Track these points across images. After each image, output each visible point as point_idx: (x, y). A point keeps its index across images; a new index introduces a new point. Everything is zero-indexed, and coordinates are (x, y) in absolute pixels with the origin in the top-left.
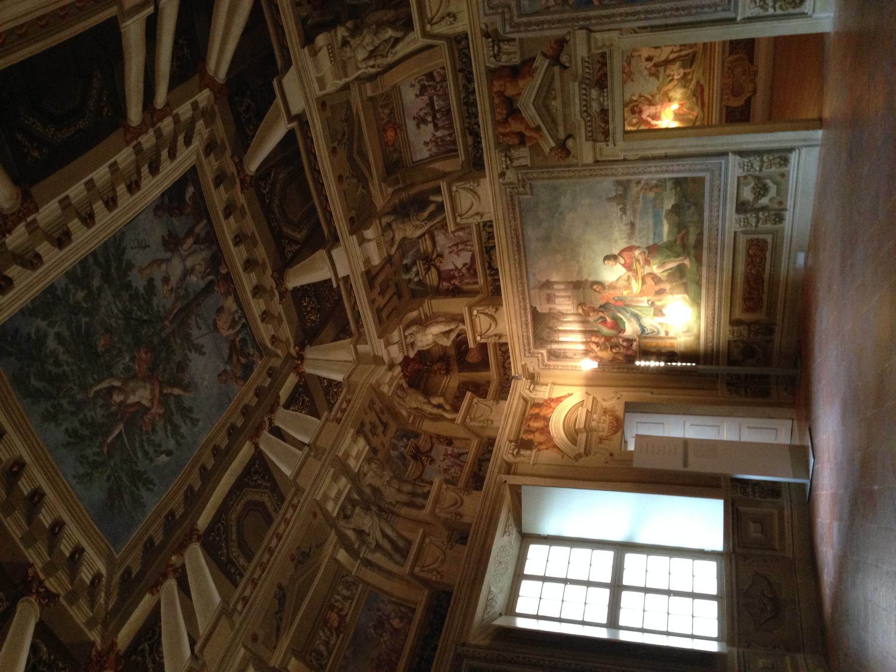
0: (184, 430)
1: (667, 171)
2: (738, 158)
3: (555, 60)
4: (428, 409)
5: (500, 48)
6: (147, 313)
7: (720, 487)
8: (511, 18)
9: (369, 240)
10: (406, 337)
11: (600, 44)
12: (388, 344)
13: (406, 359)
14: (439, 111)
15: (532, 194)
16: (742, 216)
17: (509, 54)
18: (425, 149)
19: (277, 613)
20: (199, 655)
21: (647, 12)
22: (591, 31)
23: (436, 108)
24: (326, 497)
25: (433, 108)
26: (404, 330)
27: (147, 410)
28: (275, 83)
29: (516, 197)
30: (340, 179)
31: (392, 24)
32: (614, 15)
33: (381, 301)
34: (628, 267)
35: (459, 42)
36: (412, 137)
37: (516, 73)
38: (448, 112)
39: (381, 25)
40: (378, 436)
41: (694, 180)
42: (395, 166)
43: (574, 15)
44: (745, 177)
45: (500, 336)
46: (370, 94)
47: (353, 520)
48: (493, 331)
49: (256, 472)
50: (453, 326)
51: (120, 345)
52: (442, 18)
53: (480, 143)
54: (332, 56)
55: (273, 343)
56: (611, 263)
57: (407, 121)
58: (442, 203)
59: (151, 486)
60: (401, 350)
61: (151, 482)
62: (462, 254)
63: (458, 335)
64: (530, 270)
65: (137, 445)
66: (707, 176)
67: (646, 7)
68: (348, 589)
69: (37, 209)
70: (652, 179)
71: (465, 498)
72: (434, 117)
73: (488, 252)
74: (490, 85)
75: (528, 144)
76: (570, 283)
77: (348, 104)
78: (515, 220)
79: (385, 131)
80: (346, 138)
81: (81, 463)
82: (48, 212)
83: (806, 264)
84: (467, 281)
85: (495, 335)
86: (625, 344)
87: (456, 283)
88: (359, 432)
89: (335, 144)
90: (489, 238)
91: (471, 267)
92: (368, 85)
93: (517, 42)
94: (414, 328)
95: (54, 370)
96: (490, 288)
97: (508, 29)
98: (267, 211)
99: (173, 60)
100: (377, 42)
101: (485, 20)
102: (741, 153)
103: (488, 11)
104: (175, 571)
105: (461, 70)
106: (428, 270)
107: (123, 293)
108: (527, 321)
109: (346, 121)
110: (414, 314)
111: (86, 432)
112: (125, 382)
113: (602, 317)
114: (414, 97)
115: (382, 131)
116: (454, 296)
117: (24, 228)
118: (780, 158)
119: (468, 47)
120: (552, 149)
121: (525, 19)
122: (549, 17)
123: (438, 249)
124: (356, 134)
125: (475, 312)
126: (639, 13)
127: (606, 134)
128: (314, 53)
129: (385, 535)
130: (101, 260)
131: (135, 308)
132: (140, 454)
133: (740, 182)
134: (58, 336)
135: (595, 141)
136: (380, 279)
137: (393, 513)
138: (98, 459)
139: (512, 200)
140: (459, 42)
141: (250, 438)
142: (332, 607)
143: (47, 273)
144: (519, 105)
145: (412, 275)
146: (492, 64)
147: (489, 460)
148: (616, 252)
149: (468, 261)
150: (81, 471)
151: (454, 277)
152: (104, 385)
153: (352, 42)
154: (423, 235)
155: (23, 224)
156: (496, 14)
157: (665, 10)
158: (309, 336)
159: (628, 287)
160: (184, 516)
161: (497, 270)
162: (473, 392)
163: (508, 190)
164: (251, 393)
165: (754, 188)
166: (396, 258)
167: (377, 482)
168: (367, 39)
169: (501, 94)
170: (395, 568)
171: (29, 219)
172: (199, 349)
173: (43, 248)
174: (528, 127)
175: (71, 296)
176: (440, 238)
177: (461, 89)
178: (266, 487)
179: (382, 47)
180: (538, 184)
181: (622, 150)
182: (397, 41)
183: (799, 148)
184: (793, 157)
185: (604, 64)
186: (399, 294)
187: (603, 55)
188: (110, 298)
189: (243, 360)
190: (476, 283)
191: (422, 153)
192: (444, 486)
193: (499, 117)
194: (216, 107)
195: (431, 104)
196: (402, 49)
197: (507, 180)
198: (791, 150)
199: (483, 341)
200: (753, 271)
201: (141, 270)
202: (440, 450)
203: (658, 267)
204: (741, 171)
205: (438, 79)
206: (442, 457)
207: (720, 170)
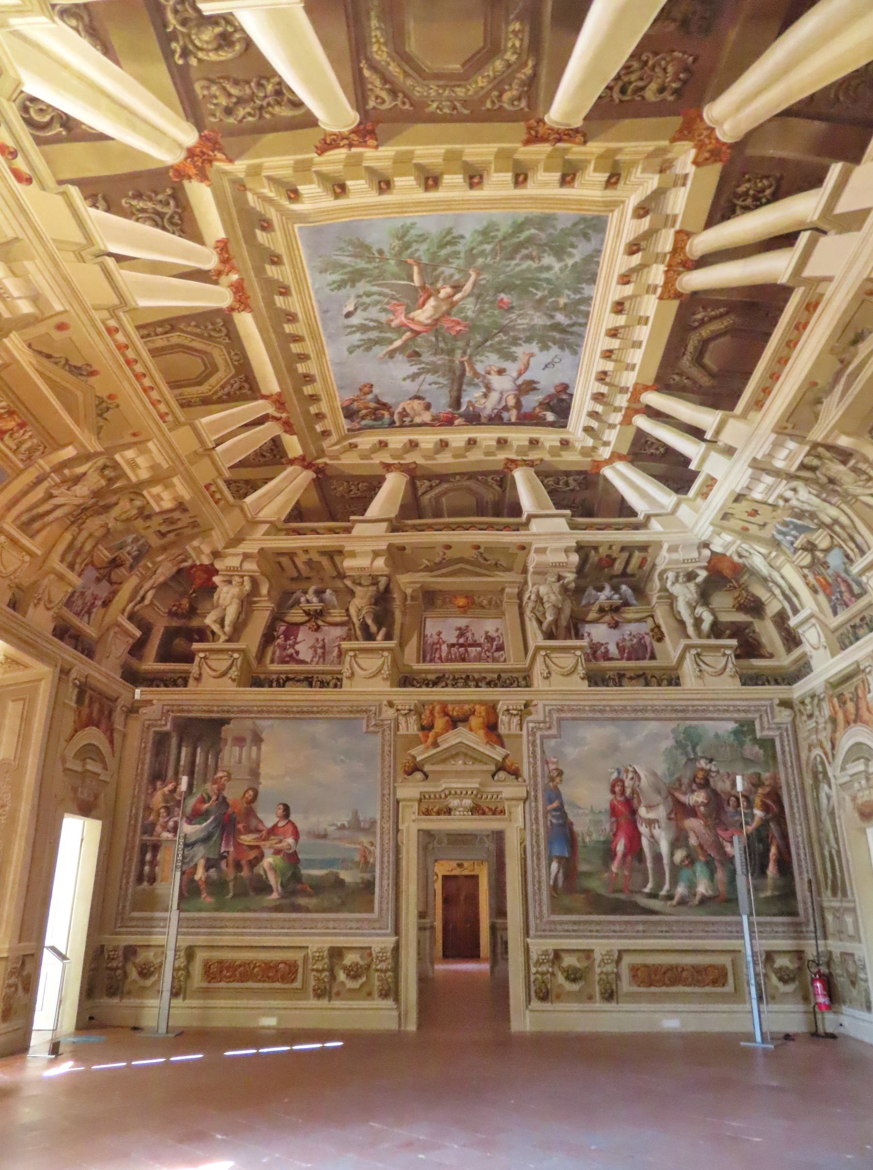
0: (358, 336)
1: (382, 873)
2: (392, 946)
3: (501, 767)
4: (147, 586)
5: (515, 715)
6: (491, 345)
7: (20, 941)
8: (541, 729)
9: (373, 561)
10: (242, 577)
11: (513, 810)
12: (246, 556)
13: (216, 572)
14: (466, 651)
15: (367, 732)
16: (326, 953)
17: (509, 723)
18: (434, 632)
19: (67, 360)
20: (100, 259)
21: (539, 854)
22: (525, 801)
23: (469, 649)
24: (146, 451)
25: (471, 645)
26: (251, 577)
27: (408, 311)
28: (568, 512)
29: (365, 716)
30: (448, 547)
31: (556, 622)
32: (537, 823)
33: (300, 560)
34: (273, 830)
35: (525, 678)
36: (450, 621)
37: (491, 728)
38: (463, 660)
39: (559, 611)
40: (160, 524)
41: (372, 901)
42: (430, 598)
43: (540, 786)
44: (370, 955)
45: (198, 679)
46: (507, 590)
47: (96, 475)
48: (206, 670)
50: (227, 629)
52: (547, 667)
53: (427, 685)
54: (555, 565)
55: (350, 444)
56: (280, 811)
57: (467, 620)
58: (374, 640)
59: (335, 285)
60: (229, 569)
61: (339, 288)
62: (311, 652)
63: (213, 633)
64: (278, 722)
66: (375, 915)
67: (543, 853)
68: (28, 449)
69: (661, 298)
70: (375, 858)
71: (51, 613)
72: (461, 645)
73: (306, 679)
74: (482, 703)
75: (420, 734)
76: (258, 765)
77: (509, 569)
78: (338, 712)
79: (466, 597)
80: (484, 560)
81: (420, 236)
82: (650, 305)
83: (263, 1028)
84: (278, 653)
85: (200, 674)
86: (171, 824)
87: (279, 641)
88: (181, 506)
89: (482, 550)
90: (322, 682)
91: (293, 659)
92: (516, 591)
93: (519, 732)
94: (247, 587)
95: (524, 252)
96: (262, 677)
97: (531, 725)
98: (471, 476)
99: (657, 439)
100: (547, 605)
101: (540, 706)
102: (396, 949)
103: (547, 708)
104: (219, 273)
105: (499, 677)
106: (307, 613)
107: (528, 334)
108: (212, 712)
109: (496, 564)
110: (264, 590)
111: (443, 252)
112: (453, 305)
113: (210, 798)
114: (487, 629)
115: (469, 596)
116: (264, 635)
118: (389, 989)
119: (518, 686)
120: (414, 757)
121: (538, 742)
122: (539, 763)
123: (326, 628)
124: (478, 570)
125: (236, 655)
126: (539, 846)
127: (427, 813)
128: (567, 551)
129: (58, 507)
130: (575, 329)
131: (504, 338)
132: (375, 289)
133: (366, 951)
134: (549, 268)
135: (420, 801)
136: (325, 562)
137: (73, 523)
138: (409, 251)
139: (362, 711)
140: (524, 679)
142: (22, 425)
144: (461, 729)
145: (311, 596)
146: (501, 707)
147: (76, 648)
148: (293, 817)
149: (301, 656)
150: (413, 232)
151: (287, 638)
152: (468, 287)
153: (558, 584)
154: (349, 615)
156: (545, 716)
157: (539, 871)
158: (323, 478)
159: (248, 831)
160: (270, 304)
161: (283, 686)
162: (139, 639)
163: (373, 708)
165: (357, 964)
166: (339, 584)
167: (115, 512)
168: (553, 598)
169: (473, 713)
170: (15, 512)
174: (438, 735)
176: (338, 632)
177: (484, 675)
179: (541, 608)
180: (378, 738)
181: (408, 828)
182: (540, 623)
183: (398, 1008)
184: (389, 1003)
185: (494, 813)
186: (299, 578)
187: (502, 812)
189: (364, 412)
190: (272, 662)
191: (431, 628)
192: (70, 590)
193: (450, 707)
194: (589, 459)
195: (475, 644)
196: (532, 626)
197: (384, 708)
198: (397, 1000)
199: (197, 659)
200: (256, 970)
201: (532, 355)
202: (103, 590)
203: (271, 864)
204: (378, 950)
205: (496, 654)
206: (96, 593)
207: (380, 928)
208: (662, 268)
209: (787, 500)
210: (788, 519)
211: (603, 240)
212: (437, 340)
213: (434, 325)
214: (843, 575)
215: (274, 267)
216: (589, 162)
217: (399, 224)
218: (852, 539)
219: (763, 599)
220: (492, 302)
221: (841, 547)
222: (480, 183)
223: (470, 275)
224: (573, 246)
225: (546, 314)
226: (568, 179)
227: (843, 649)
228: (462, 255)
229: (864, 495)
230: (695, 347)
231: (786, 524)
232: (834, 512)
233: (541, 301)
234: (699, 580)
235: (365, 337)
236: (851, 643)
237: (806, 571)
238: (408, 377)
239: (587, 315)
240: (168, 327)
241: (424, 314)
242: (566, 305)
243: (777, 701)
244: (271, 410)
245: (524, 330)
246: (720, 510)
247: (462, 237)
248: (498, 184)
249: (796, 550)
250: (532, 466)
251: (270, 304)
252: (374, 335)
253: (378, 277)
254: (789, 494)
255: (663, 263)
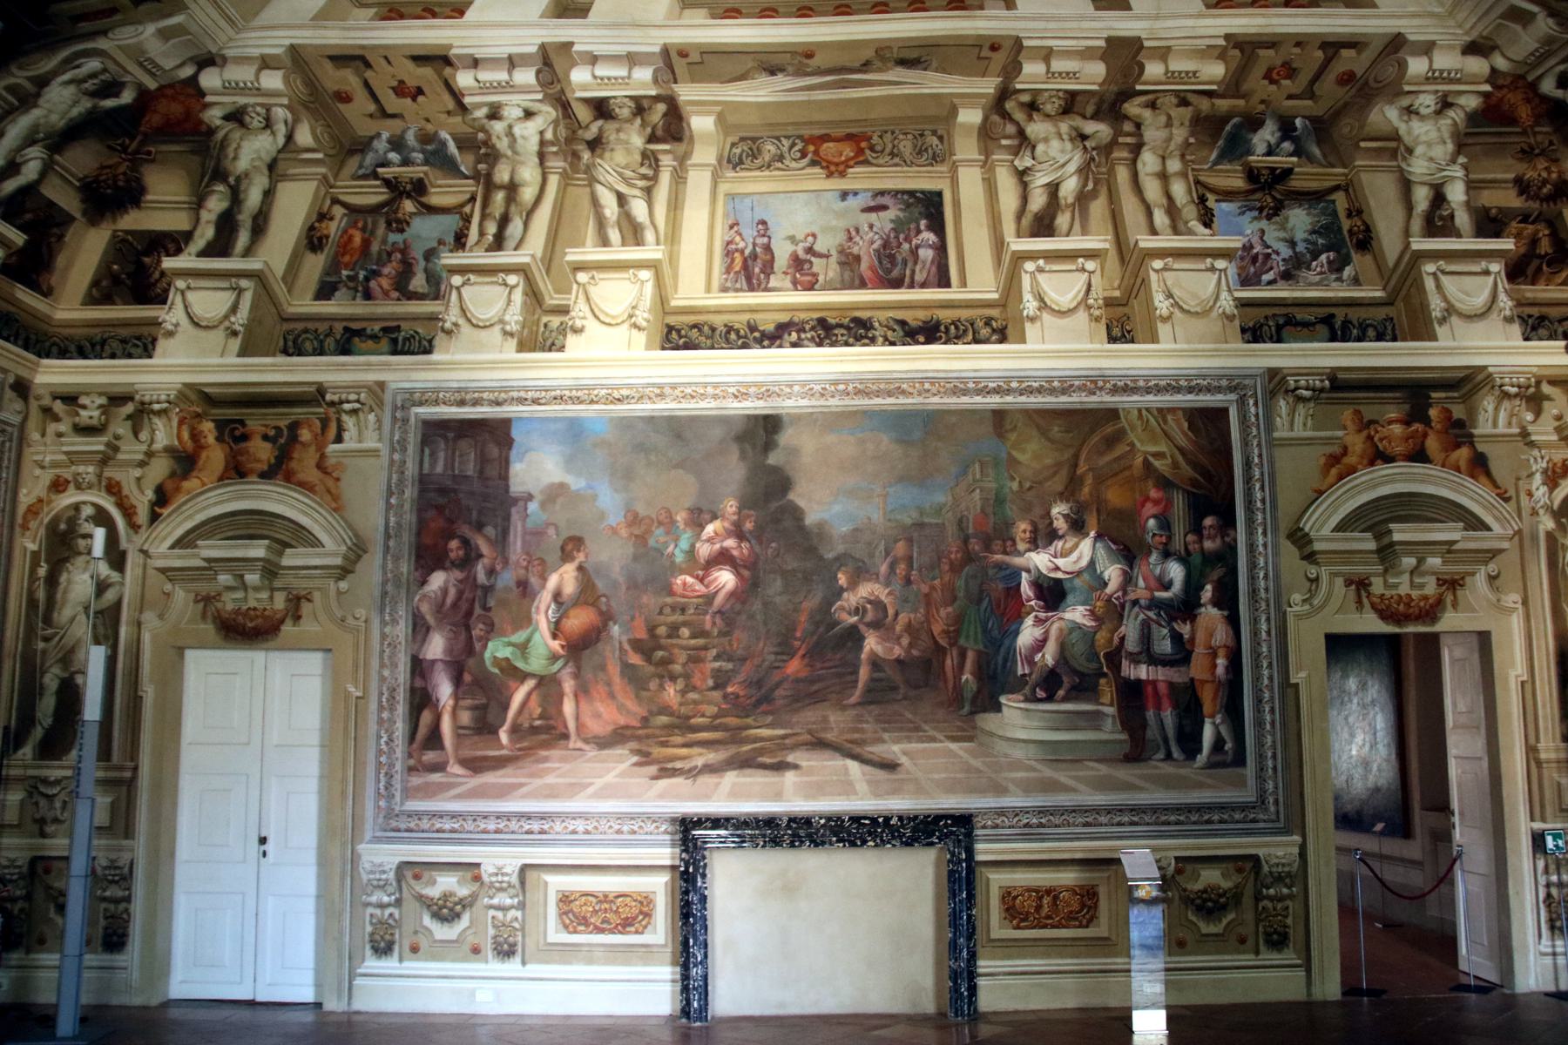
209: (495, 114)
210: (444, 135)
214: (417, 253)
218: (504, 221)
219: (149, 197)
221: (467, 220)
227: (286, 352)
229: (611, 189)
231: (426, 138)
232: (529, 174)
234: (109, 103)
236: (321, 352)
237: (338, 211)
243: (11, 380)
246: (363, 47)
249: (375, 176)
254: (512, 113)
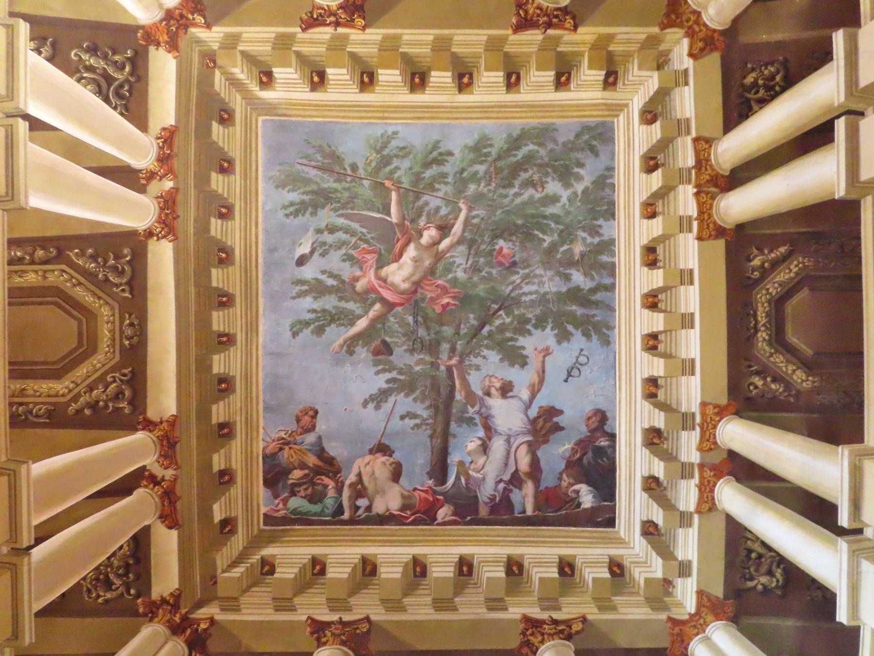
0: (308, 302)
6: (490, 335)
49: (118, 395)
51: (483, 273)
65: (355, 226)
69: (700, 238)
82: (689, 251)
117: (690, 214)
130: (599, 296)
141: (173, 422)
143: (629, 216)
155: (695, 215)
164: (237, 464)
171: (695, 224)
172: (379, 398)
173: (656, 227)
175: (584, 235)
178: (75, 399)
188: (546, 288)
208: (691, 189)
211: (613, 154)
212: (416, 322)
213: (412, 297)
215: (221, 177)
216: (581, 54)
217: (379, 132)
220: (490, 253)
222: (470, 84)
223: (460, 210)
224: (581, 165)
225: (559, 274)
226: (563, 79)
228: (450, 179)
230: (768, 315)
233: (552, 249)
235: (317, 305)
238: (372, 398)
239: (611, 270)
240: (54, 252)
241: (400, 273)
242: (583, 255)
244: (150, 461)
245: (532, 303)
247: (450, 154)
248: (489, 85)
250: (569, 638)
251: (203, 228)
252: (330, 302)
253: (345, 205)
255: (690, 182)
